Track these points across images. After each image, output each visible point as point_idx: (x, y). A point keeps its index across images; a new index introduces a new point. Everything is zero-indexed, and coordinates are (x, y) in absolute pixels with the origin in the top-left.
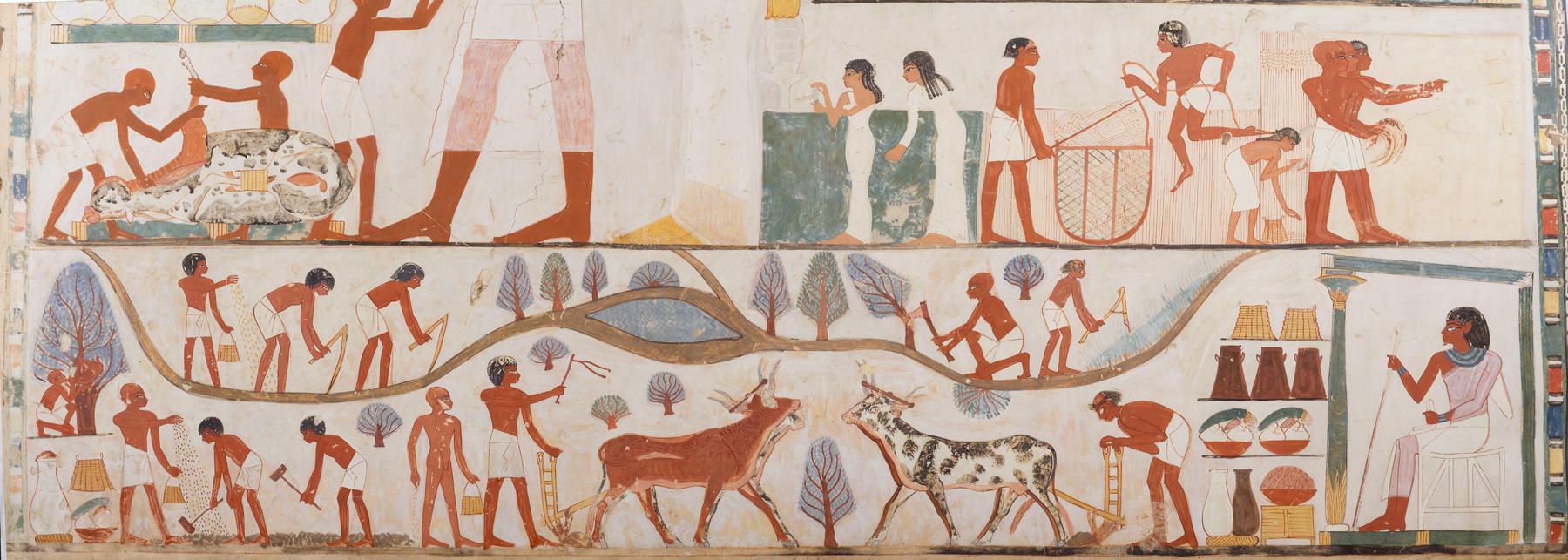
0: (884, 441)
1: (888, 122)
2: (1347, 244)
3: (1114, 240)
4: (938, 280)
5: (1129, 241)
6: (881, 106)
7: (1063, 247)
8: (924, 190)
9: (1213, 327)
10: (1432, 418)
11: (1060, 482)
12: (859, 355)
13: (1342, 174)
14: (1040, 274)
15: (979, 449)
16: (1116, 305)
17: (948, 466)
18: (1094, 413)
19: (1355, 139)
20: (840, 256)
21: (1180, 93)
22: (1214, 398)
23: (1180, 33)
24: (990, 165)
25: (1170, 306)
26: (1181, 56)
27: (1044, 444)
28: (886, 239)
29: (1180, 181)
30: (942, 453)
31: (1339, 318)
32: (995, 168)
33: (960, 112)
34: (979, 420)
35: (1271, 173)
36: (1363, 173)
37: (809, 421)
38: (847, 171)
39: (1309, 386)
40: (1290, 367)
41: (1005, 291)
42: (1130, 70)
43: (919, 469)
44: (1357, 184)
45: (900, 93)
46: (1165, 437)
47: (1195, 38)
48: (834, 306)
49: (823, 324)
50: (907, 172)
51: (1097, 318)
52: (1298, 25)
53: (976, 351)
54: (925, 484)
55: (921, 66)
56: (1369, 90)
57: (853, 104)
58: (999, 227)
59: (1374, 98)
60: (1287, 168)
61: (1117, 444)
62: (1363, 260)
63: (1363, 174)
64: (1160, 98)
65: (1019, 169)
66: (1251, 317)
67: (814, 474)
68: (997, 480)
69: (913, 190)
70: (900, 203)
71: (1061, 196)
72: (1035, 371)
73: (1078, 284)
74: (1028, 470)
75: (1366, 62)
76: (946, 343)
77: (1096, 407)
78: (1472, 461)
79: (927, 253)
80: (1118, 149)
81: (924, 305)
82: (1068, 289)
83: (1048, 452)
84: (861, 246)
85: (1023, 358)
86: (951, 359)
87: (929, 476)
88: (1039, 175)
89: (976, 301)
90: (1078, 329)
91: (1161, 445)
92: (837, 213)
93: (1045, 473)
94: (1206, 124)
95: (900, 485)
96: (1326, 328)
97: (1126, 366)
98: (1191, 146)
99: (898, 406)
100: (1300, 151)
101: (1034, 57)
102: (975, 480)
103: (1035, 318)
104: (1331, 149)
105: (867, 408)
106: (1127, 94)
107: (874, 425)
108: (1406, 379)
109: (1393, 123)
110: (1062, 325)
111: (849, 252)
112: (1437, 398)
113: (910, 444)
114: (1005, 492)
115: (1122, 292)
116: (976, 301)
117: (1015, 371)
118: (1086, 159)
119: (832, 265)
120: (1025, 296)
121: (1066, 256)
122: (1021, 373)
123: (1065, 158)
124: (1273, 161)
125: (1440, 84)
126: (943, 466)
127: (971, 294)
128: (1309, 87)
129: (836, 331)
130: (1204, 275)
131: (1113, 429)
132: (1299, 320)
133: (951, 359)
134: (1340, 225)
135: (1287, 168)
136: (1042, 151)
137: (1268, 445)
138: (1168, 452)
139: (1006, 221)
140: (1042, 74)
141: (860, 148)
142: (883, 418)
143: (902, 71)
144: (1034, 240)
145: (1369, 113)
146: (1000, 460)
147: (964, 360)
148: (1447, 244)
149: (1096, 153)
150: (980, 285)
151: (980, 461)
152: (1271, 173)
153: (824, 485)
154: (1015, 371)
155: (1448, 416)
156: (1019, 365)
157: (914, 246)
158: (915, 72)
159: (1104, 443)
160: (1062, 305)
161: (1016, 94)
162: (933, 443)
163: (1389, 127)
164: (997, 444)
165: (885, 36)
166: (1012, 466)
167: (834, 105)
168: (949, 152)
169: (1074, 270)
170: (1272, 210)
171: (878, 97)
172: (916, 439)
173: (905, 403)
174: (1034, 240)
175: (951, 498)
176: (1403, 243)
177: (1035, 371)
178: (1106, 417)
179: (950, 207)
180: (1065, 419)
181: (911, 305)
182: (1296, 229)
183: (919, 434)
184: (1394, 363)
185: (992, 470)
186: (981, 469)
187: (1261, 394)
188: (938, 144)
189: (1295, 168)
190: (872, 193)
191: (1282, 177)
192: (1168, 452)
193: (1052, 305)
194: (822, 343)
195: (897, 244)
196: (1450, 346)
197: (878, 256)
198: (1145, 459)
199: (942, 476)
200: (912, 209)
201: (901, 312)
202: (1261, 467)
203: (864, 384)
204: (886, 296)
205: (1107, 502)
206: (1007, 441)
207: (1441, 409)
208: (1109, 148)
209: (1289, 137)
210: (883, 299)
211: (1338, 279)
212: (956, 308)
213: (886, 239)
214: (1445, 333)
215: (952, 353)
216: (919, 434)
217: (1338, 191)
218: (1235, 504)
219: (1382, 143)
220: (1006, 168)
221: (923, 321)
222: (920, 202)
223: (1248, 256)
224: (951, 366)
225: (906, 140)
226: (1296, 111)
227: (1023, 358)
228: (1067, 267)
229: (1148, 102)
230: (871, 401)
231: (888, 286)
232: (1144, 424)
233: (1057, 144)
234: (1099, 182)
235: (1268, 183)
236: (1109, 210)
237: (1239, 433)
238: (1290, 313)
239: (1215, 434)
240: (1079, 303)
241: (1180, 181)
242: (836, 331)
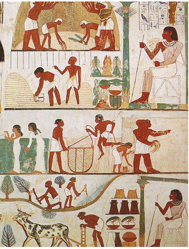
0: (24, 225)
1: (24, 141)
2: (144, 173)
3: (83, 172)
4: (37, 183)
5: (88, 172)
6: (22, 137)
7: (70, 174)
8: (34, 159)
9: (110, 195)
10: (167, 219)
11: (69, 236)
12: (17, 202)
13: (142, 154)
14: (64, 181)
15: (48, 227)
16: (84, 189)
17: (40, 232)
18: (78, 218)
19: (147, 145)
20: (12, 176)
21: (101, 134)
22: (109, 214)
23: (101, 117)
24: (51, 152)
25: (98, 189)
26: (102, 124)
27: (65, 226)
28: (24, 172)
29: (101, 156)
30: (39, 228)
31: (142, 193)
32: (52, 153)
33: (43, 139)
34: (48, 219)
35: (125, 154)
36: (148, 155)
37: (4, 220)
38: (13, 154)
39: (135, 210)
40: (130, 205)
41: (55, 186)
42: (88, 127)
43: (33, 232)
44: (147, 157)
45: (27, 133)
46: (97, 224)
47: (105, 119)
48: (10, 190)
49: (7, 194)
50: (29, 154)
51: (79, 193)
52: (132, 116)
53: (48, 201)
54: (34, 236)
55: (33, 127)
56: (151, 132)
57: (15, 136)
58: (53, 169)
59: (152, 135)
60: (129, 153)
61: (85, 226)
62: (148, 177)
63: (148, 155)
64: (96, 135)
65: (58, 154)
66: (119, 192)
67: (5, 233)
68: (53, 235)
69: (31, 159)
70: (27, 162)
71: (69, 160)
72: (63, 207)
73: (74, 184)
74: (61, 232)
75: (150, 125)
76: (39, 199)
77: (79, 216)
78: (177, 230)
79: (35, 176)
80: (84, 148)
81: (34, 189)
82: (71, 185)
83: (66, 228)
84: (17, 174)
85: (60, 203)
86: (41, 203)
87: (35, 234)
88: (64, 155)
89: (47, 188)
90: (74, 195)
91: (96, 226)
92: (11, 165)
93: (66, 233)
94: (107, 141)
95: (28, 237)
96: (139, 195)
97: (87, 205)
98: (103, 147)
99: (27, 216)
100: (132, 149)
101: (63, 125)
102: (47, 235)
103: (63, 193)
104: (140, 148)
105: (19, 216)
106: (87, 134)
107: (21, 221)
108: (160, 208)
109: (157, 141)
110: (70, 194)
111: (14, 175)
112: (169, 213)
113: (30, 226)
114: (55, 238)
115: (86, 186)
116: (47, 188)
117: (58, 207)
118: (76, 151)
119: (9, 178)
120: (60, 187)
121: (71, 176)
122: (59, 207)
123: (70, 150)
124: (125, 152)
125: (169, 131)
126: (39, 232)
127: (46, 186)
128: (135, 132)
129: (11, 196)
130: (107, 181)
131: (83, 222)
132: (132, 193)
133: (41, 203)
134: (143, 168)
135: (129, 153)
136: (64, 149)
137: (124, 226)
138: (98, 228)
139: (55, 167)
140: (65, 129)
141: (17, 149)
142: (23, 219)
143: (28, 128)
144: (62, 172)
145: (150, 138)
146: (54, 230)
147: (44, 204)
148: (170, 173)
149: (78, 149)
150: (48, 184)
151: (49, 230)
152: (125, 154)
153: (8, 237)
154: (58, 207)
155: (171, 218)
156: (59, 205)
157: (31, 174)
158: (31, 127)
159: (81, 226)
160: (70, 189)
161: (58, 134)
162: (36, 226)
163: (155, 142)
164: (53, 226)
165: (23, 119)
166: (57, 232)
167: (10, 137)
168: (40, 149)
169: (73, 180)
170: (125, 164)
171: (22, 135)
172: (31, 225)
173: (29, 215)
174: (62, 172)
175: (41, 240)
176: (159, 173)
177: (63, 207)
178: (82, 219)
179: (40, 164)
180: (71, 220)
181: (30, 189)
182: (131, 169)
183: (32, 223)
184: (157, 204)
185: (52, 233)
186: (49, 232)
187: (122, 213)
188: (37, 147)
189: (131, 153)
190: (20, 160)
191: (127, 156)
192: (98, 228)
193: (67, 189)
194: (7, 199)
195: (27, 173)
196: (172, 200)
197: (21, 176)
198: (94, 229)
199: (38, 234)
200: (30, 164)
201: (28, 191)
202: (122, 232)
203: (18, 210)
204: (24, 187)
205: (82, 241)
206: (55, 225)
207: (170, 216)
208: (82, 148)
209: (129, 145)
210: (23, 188)
211: (142, 182)
212: (42, 190)
213: (24, 172)
214: (170, 196)
215: (41, 202)
216: (32, 223)
217: (142, 159)
218: (115, 241)
219: (154, 147)
220: (55, 153)
221: (34, 193)
222: (32, 162)
223: (118, 176)
224: (40, 205)
225: (29, 146)
226: (130, 138)
227: (60, 203)
228: (71, 179)
229: (93, 136)
230: (20, 214)
231: (24, 185)
232: (92, 221)
233: (69, 147)
234: (79, 157)
235: (124, 157)
236: (82, 164)
237: (116, 223)
238: (129, 191)
239: (110, 223)
240: (74, 189)
241: (101, 156)
242: (11, 196)
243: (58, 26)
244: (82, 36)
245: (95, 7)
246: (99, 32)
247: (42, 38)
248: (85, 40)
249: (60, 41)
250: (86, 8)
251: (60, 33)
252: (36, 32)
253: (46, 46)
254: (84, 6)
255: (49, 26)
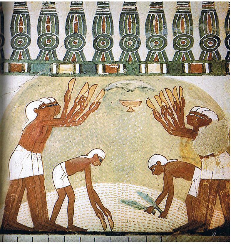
243: (94, 170)
244: (154, 194)
245: (186, 121)
246: (197, 185)
247: (51, 198)
248: (162, 206)
249: (99, 208)
250: (162, 123)
251: (99, 188)
252: (37, 182)
253: (62, 220)
254: (159, 119)
255: (72, 168)
